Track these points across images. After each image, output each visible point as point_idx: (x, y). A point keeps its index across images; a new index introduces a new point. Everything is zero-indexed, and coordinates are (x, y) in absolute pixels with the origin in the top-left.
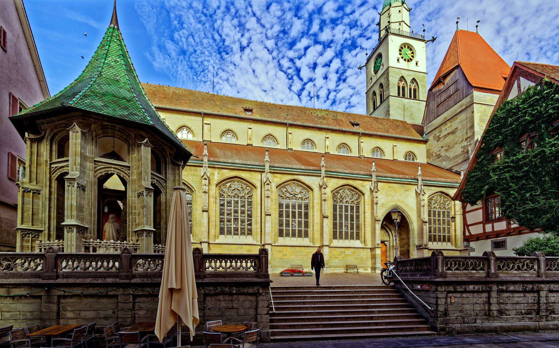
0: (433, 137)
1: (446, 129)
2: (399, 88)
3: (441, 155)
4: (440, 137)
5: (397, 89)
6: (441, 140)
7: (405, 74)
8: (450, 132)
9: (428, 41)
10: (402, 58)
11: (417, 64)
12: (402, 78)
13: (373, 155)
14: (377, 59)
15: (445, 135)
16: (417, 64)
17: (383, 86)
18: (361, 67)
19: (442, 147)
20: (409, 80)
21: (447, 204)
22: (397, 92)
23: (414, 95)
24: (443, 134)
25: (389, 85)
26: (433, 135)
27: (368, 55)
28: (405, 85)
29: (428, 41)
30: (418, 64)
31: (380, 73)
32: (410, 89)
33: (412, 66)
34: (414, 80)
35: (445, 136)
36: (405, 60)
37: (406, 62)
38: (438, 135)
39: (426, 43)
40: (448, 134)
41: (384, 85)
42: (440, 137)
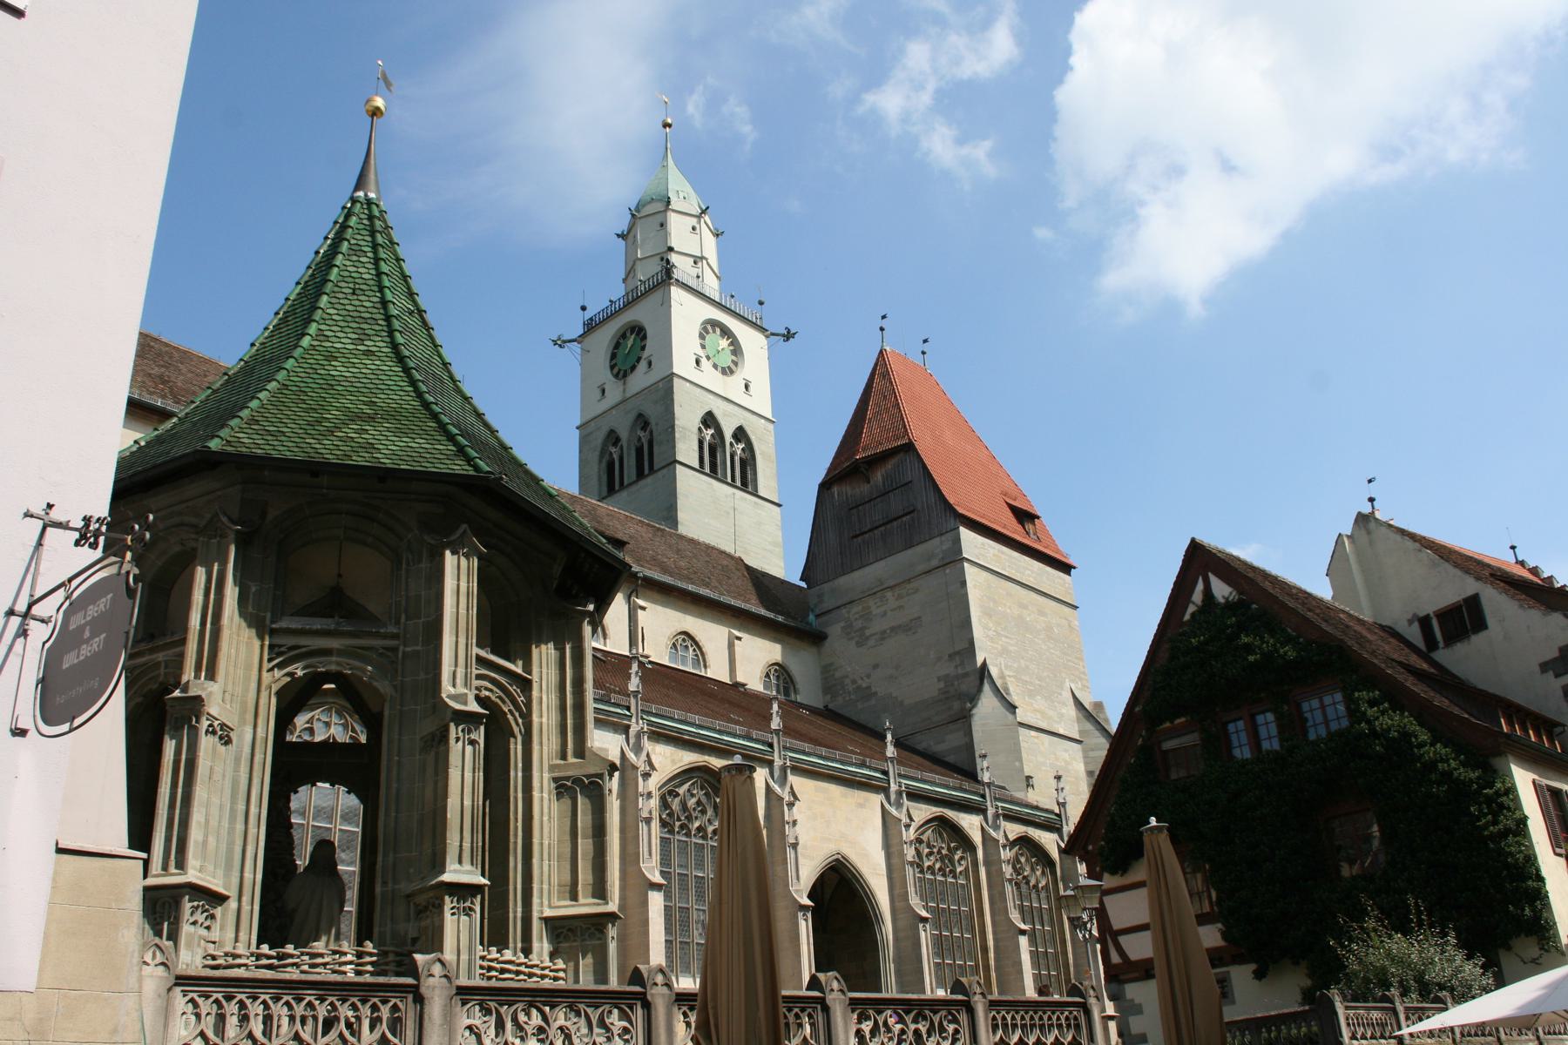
0: (843, 628)
1: (885, 614)
2: (701, 443)
3: (873, 690)
4: (868, 632)
6: (872, 642)
7: (720, 410)
8: (900, 626)
9: (773, 334)
10: (708, 358)
11: (747, 387)
12: (709, 420)
13: (673, 657)
14: (624, 336)
15: (885, 632)
16: (747, 387)
18: (565, 342)
19: (876, 666)
21: (957, 857)
22: (696, 455)
23: (746, 479)
24: (877, 626)
25: (673, 427)
26: (842, 624)
27: (589, 314)
29: (773, 334)
33: (731, 387)
34: (740, 434)
35: (883, 636)
36: (715, 366)
37: (718, 374)
38: (858, 624)
39: (767, 337)
40: (893, 629)
41: (653, 422)
42: (868, 632)
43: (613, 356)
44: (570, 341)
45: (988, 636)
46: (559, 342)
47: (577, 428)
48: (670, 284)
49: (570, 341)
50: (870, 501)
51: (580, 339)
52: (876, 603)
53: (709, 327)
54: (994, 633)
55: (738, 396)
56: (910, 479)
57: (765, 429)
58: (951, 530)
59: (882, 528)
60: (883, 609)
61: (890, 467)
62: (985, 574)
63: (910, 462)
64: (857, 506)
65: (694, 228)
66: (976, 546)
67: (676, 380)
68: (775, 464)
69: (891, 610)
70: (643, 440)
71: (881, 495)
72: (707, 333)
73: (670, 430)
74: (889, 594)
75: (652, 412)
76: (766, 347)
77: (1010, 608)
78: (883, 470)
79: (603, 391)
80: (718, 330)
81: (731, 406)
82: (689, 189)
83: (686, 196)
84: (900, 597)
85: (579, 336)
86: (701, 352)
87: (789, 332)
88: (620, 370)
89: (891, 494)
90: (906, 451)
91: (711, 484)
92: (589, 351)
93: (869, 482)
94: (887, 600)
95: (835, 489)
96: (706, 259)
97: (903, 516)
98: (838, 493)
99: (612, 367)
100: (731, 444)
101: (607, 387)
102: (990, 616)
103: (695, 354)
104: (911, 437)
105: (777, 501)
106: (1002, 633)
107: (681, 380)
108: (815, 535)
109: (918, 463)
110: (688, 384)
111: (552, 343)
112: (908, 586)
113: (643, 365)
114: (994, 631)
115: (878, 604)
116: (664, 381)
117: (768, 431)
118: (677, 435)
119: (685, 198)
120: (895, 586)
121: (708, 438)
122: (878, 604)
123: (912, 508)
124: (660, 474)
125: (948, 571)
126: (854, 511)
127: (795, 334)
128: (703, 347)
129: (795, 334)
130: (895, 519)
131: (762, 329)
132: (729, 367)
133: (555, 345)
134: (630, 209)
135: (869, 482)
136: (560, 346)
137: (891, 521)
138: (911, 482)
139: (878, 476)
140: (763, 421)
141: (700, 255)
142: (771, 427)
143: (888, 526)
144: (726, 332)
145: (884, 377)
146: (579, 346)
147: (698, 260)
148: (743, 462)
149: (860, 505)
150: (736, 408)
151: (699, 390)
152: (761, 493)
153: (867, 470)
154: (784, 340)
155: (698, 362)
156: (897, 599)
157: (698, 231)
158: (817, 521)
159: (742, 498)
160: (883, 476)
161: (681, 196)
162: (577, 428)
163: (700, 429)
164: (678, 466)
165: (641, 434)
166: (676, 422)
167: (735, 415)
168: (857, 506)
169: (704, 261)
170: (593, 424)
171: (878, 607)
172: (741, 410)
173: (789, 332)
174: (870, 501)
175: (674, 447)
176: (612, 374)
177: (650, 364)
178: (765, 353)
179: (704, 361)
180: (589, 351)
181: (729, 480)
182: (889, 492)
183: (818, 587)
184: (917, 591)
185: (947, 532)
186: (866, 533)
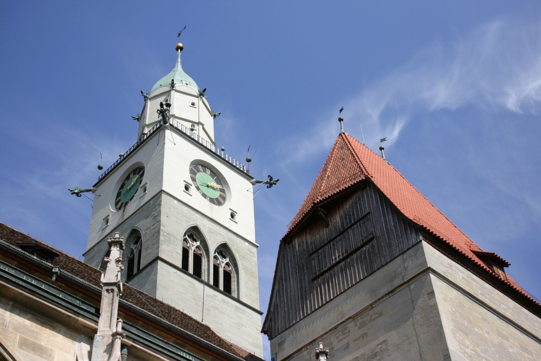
2: (185, 252)
5: (180, 251)
7: (205, 227)
9: (258, 182)
14: (128, 178)
16: (232, 216)
17: (139, 238)
20: (212, 248)
25: (158, 232)
28: (202, 252)
30: (237, 217)
31: (132, 208)
32: (216, 269)
36: (204, 196)
37: (206, 202)
39: (253, 184)
41: (142, 233)
43: (119, 194)
44: (88, 191)
45: (465, 353)
46: (76, 191)
47: (83, 255)
48: (166, 128)
49: (88, 191)
50: (329, 242)
51: (95, 188)
52: (337, 338)
53: (200, 167)
54: (474, 353)
55: (225, 220)
56: (368, 211)
57: (248, 250)
58: (413, 246)
59: (343, 263)
60: (345, 342)
61: (348, 207)
62: (455, 293)
63: (368, 197)
64: (317, 251)
65: (193, 104)
66: (442, 264)
67: (164, 196)
68: (257, 280)
69: (353, 341)
70: (135, 251)
71: (339, 235)
72: (199, 171)
73: (156, 234)
74: (351, 325)
75: (142, 225)
76: (252, 190)
77: (488, 333)
78: (342, 212)
79: (107, 222)
80: (208, 171)
81: (218, 227)
82: (190, 80)
83: (188, 83)
84: (363, 325)
85: (94, 186)
86: (190, 181)
87: (271, 179)
88: (122, 203)
89: (350, 231)
90: (364, 188)
91: (193, 284)
92: (100, 196)
93: (327, 226)
94: (349, 331)
95: (296, 242)
96: (203, 125)
97: (362, 246)
98: (299, 246)
99: (116, 204)
100: (215, 257)
101: (110, 218)
102: (467, 334)
103: (185, 181)
104: (366, 174)
105: (258, 308)
106: (482, 354)
107: (169, 197)
108: (276, 287)
109: (375, 195)
110: (176, 202)
111: (70, 193)
112: (371, 312)
113: (140, 191)
114: (472, 350)
115: (341, 337)
116: (153, 199)
117: (252, 252)
118: (161, 238)
119: (187, 84)
120: (357, 314)
121: (193, 248)
122: (341, 337)
123: (370, 237)
124: (144, 273)
125: (412, 287)
126: (315, 255)
127: (277, 181)
128: (194, 180)
129: (277, 181)
130: (355, 251)
131: (247, 176)
132: (217, 199)
133: (72, 194)
134: (142, 92)
135: (327, 226)
136: (77, 194)
137: (351, 254)
138: (369, 213)
139: (337, 219)
140: (247, 244)
141: (197, 121)
142: (254, 250)
143: (348, 260)
144: (215, 173)
145: (342, 148)
146: (94, 194)
147: (196, 125)
148: (227, 275)
149: (320, 249)
150: (222, 229)
151: (186, 208)
152: (243, 299)
153: (326, 216)
154: (268, 187)
155: (187, 188)
156: (359, 329)
157: (196, 105)
158: (279, 274)
159: (224, 301)
160: (341, 218)
161: (184, 83)
162: (83, 255)
163: (185, 240)
164: (160, 262)
165: (133, 246)
166: (162, 228)
167: (220, 234)
168: (317, 251)
169: (201, 126)
170: (96, 248)
171: (339, 341)
172: (226, 232)
173: (271, 179)
174: (329, 242)
175: (158, 247)
176: (116, 208)
177: (145, 190)
178: (251, 196)
179: (193, 189)
180: (100, 196)
181: (212, 283)
182: (347, 230)
183: (279, 337)
184: (381, 314)
185: (408, 249)
186: (326, 272)
